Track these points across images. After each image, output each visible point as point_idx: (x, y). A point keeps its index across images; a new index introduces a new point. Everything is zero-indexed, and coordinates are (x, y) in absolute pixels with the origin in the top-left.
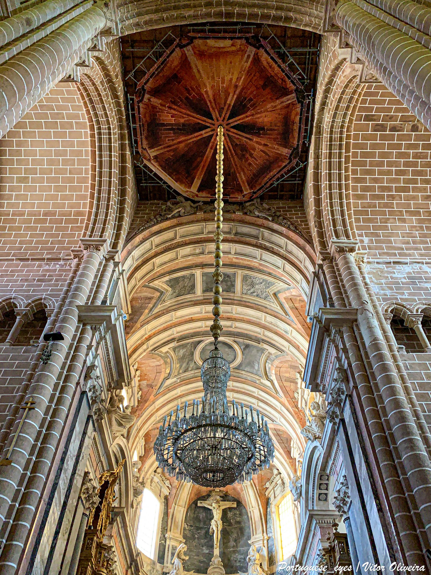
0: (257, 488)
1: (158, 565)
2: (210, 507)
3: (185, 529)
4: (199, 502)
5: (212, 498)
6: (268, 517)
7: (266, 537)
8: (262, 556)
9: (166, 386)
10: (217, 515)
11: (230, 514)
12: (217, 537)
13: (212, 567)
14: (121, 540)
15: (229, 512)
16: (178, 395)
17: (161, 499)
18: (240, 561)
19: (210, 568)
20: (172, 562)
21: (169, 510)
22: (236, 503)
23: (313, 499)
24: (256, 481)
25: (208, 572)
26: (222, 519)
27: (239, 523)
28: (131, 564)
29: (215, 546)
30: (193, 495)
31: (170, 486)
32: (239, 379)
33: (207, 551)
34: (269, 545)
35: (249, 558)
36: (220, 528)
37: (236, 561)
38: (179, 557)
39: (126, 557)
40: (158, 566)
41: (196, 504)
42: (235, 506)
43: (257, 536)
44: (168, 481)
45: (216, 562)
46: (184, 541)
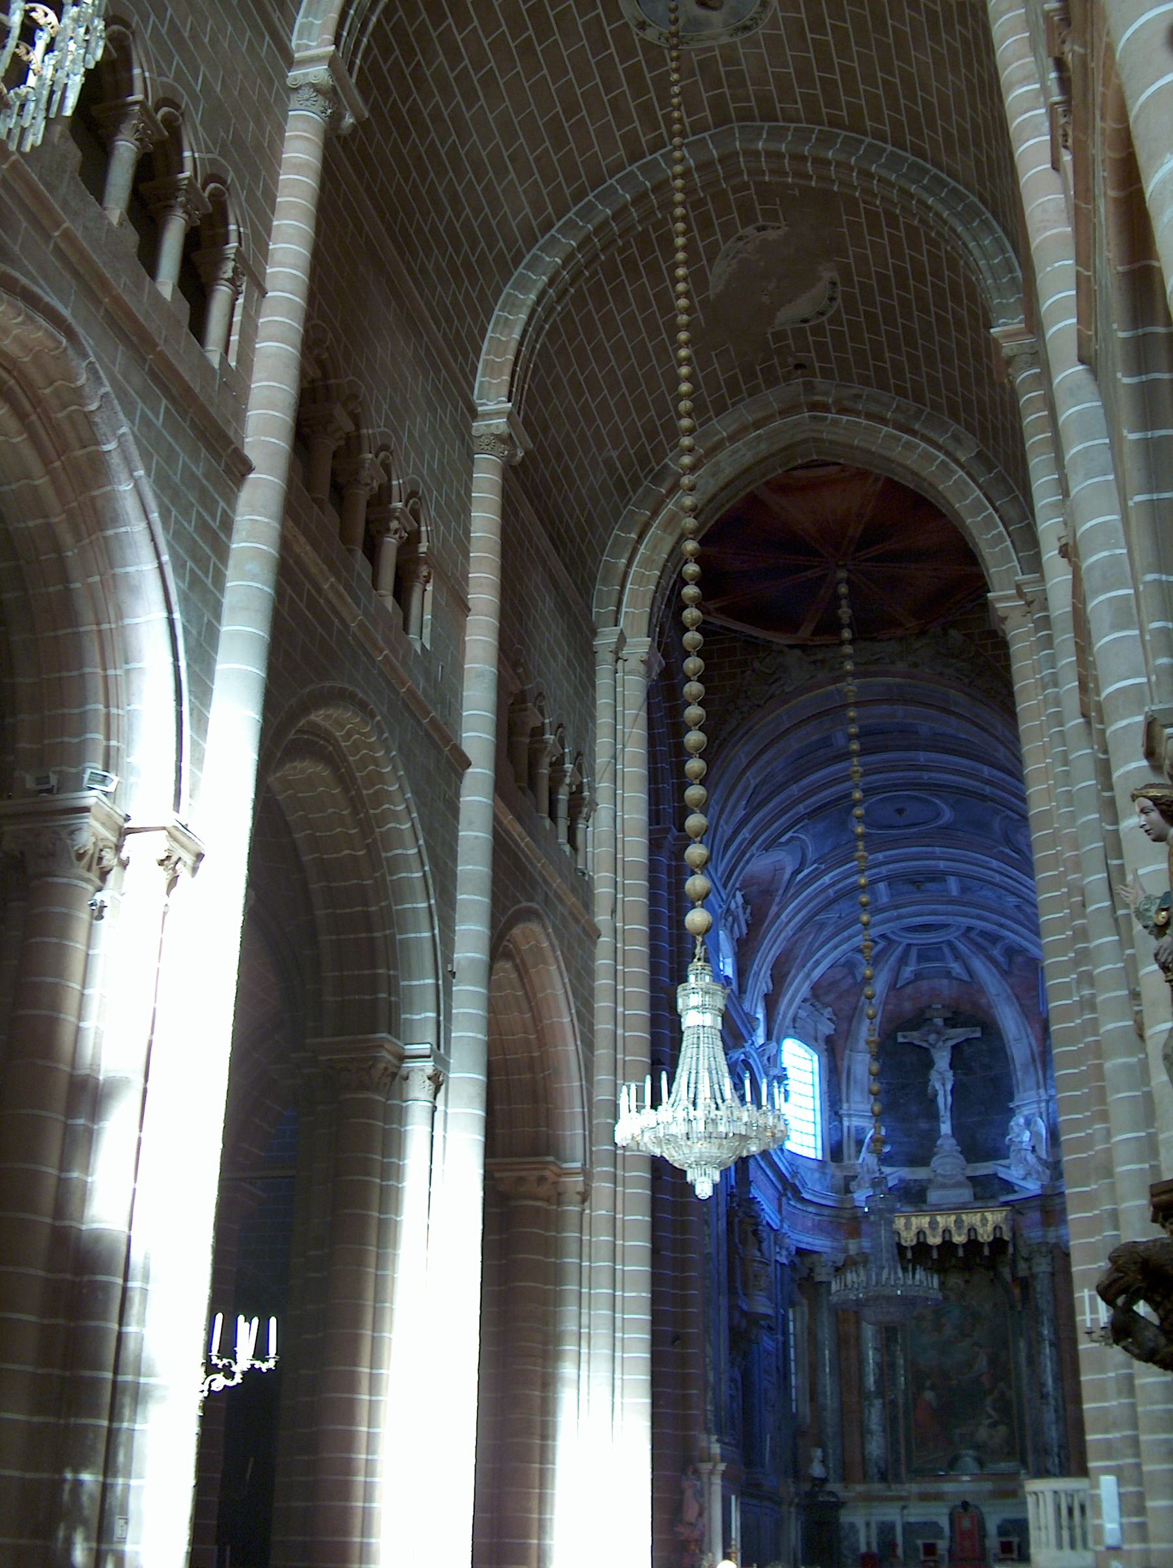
1: (833, 1164)
2: (924, 1045)
8: (1035, 1135)
10: (942, 1060)
11: (967, 1050)
12: (944, 1101)
15: (966, 1048)
19: (934, 1159)
21: (839, 1063)
22: (978, 1029)
25: (932, 1164)
26: (952, 1066)
28: (785, 1189)
36: (949, 1087)
40: (832, 1167)
41: (896, 1039)
42: (978, 1035)
44: (829, 1009)
45: (947, 1147)
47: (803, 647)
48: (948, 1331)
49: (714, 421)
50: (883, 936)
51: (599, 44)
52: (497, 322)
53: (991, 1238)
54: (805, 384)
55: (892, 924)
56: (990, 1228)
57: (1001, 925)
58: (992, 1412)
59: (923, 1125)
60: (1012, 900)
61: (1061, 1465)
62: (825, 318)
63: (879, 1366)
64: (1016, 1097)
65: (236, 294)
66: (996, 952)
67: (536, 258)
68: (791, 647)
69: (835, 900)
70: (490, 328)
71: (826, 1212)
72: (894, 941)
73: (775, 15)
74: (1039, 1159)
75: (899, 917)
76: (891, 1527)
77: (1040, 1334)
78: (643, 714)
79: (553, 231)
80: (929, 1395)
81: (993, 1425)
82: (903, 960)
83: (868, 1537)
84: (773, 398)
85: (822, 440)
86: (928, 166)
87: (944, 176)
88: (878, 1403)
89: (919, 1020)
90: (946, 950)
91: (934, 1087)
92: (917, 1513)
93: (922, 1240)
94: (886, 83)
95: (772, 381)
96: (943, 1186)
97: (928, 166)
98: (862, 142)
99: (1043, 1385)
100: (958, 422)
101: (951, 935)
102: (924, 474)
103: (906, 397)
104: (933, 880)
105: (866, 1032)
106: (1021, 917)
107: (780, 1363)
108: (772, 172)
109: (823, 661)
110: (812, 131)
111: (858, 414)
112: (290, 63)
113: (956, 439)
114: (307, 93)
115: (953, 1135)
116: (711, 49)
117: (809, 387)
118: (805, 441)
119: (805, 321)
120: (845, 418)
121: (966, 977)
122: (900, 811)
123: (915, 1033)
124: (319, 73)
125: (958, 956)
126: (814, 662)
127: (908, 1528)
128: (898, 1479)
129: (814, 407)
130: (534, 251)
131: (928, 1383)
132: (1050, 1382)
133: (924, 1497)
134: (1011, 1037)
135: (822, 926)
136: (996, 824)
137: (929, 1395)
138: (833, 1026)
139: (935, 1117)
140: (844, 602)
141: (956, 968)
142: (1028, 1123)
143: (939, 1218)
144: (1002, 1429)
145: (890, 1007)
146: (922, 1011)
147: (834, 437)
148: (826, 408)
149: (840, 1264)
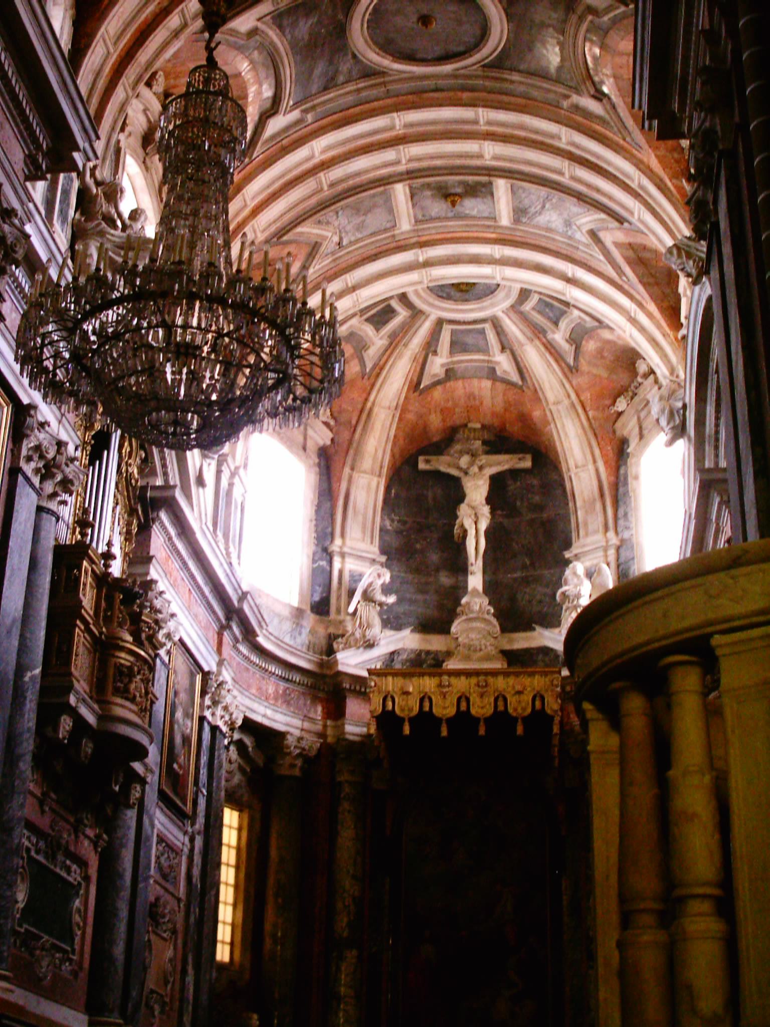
0: (591, 414)
2: (454, 472)
3: (382, 530)
4: (421, 458)
5: (458, 447)
6: (621, 490)
7: (614, 540)
9: (273, 137)
11: (513, 487)
13: (464, 617)
14: (185, 563)
15: (510, 482)
16: (316, 161)
17: (308, 457)
18: (540, 602)
20: (351, 609)
21: (335, 486)
22: (529, 457)
23: (717, 440)
24: (586, 396)
25: (453, 629)
26: (489, 500)
27: (540, 508)
28: (228, 618)
29: (470, 568)
30: (401, 442)
31: (332, 423)
32: (505, 98)
34: (622, 560)
35: (563, 594)
36: (483, 525)
37: (530, 602)
39: (208, 603)
42: (527, 463)
43: (589, 540)
46: (383, 559)
53: (529, 710)
55: (414, 276)
56: (527, 698)
59: (445, 579)
64: (574, 545)
66: (559, 337)
71: (297, 677)
72: (421, 312)
88: (351, 955)
91: (462, 526)
93: (426, 708)
107: (196, 872)
121: (515, 378)
134: (571, 463)
138: (330, 435)
139: (461, 568)
141: (504, 363)
145: (411, 416)
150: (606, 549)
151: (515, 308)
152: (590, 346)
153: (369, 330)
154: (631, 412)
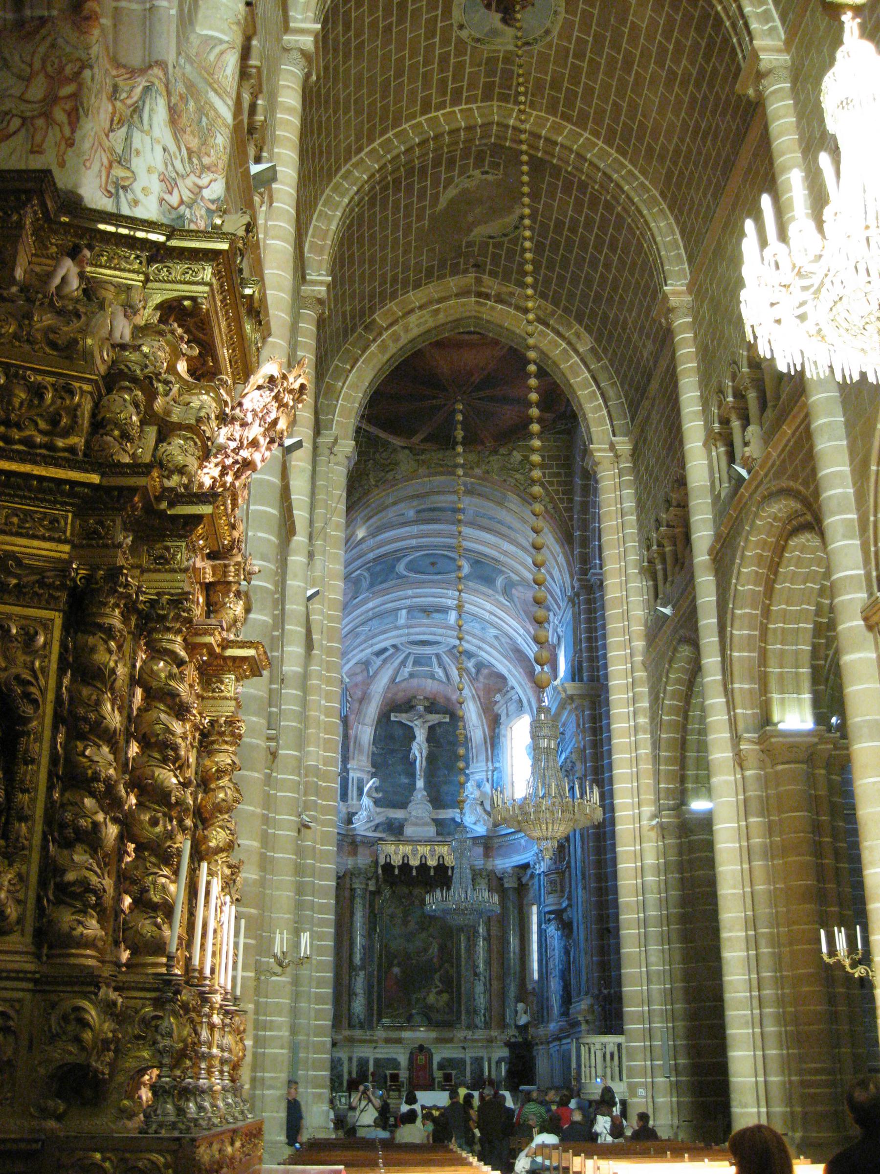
3: (373, 754)
10: (421, 735)
11: (439, 730)
24: (481, 693)
26: (429, 740)
33: (406, 781)
38: (369, 795)
41: (389, 717)
42: (448, 720)
47: (410, 449)
48: (412, 926)
49: (411, 294)
50: (394, 646)
51: (431, 33)
52: (320, 215)
54: (476, 278)
57: (480, 648)
58: (438, 984)
59: (404, 780)
60: (493, 631)
61: (486, 1022)
62: (506, 239)
63: (364, 947)
64: (471, 766)
65: (263, 202)
66: (470, 665)
67: (349, 172)
68: (404, 448)
69: (370, 619)
70: (315, 217)
73: (552, 40)
74: (485, 810)
75: (409, 634)
76: (367, 1061)
77: (478, 932)
78: (345, 495)
79: (362, 154)
80: (396, 970)
81: (439, 993)
82: (403, 663)
83: (350, 1068)
84: (453, 283)
85: (482, 319)
86: (626, 163)
87: (636, 172)
88: (362, 974)
89: (407, 706)
90: (434, 660)
92: (384, 1052)
94: (615, 103)
95: (455, 271)
96: (416, 825)
97: (626, 163)
98: (581, 135)
99: (478, 967)
100: (581, 324)
101: (441, 650)
102: (551, 355)
103: (547, 301)
104: (438, 611)
105: (372, 710)
106: (496, 643)
108: (545, 152)
109: (423, 461)
110: (548, 120)
111: (510, 305)
112: (287, 29)
113: (577, 335)
114: (296, 55)
115: (425, 789)
116: (498, 51)
117: (479, 281)
118: (470, 317)
119: (491, 237)
120: (500, 306)
122: (433, 564)
123: (404, 715)
124: (307, 42)
125: (441, 664)
126: (418, 460)
127: (377, 1061)
128: (371, 1028)
129: (479, 295)
130: (348, 166)
131: (395, 962)
132: (481, 965)
133: (388, 1041)
135: (357, 635)
136: (500, 581)
137: (396, 970)
139: (412, 775)
140: (459, 426)
141: (440, 672)
142: (479, 786)
143: (419, 848)
144: (445, 997)
146: (410, 701)
147: (489, 318)
148: (487, 296)
149: (341, 874)
150: (487, 771)
151: (450, 651)
152: (485, 671)
153: (374, 658)
154: (502, 702)
